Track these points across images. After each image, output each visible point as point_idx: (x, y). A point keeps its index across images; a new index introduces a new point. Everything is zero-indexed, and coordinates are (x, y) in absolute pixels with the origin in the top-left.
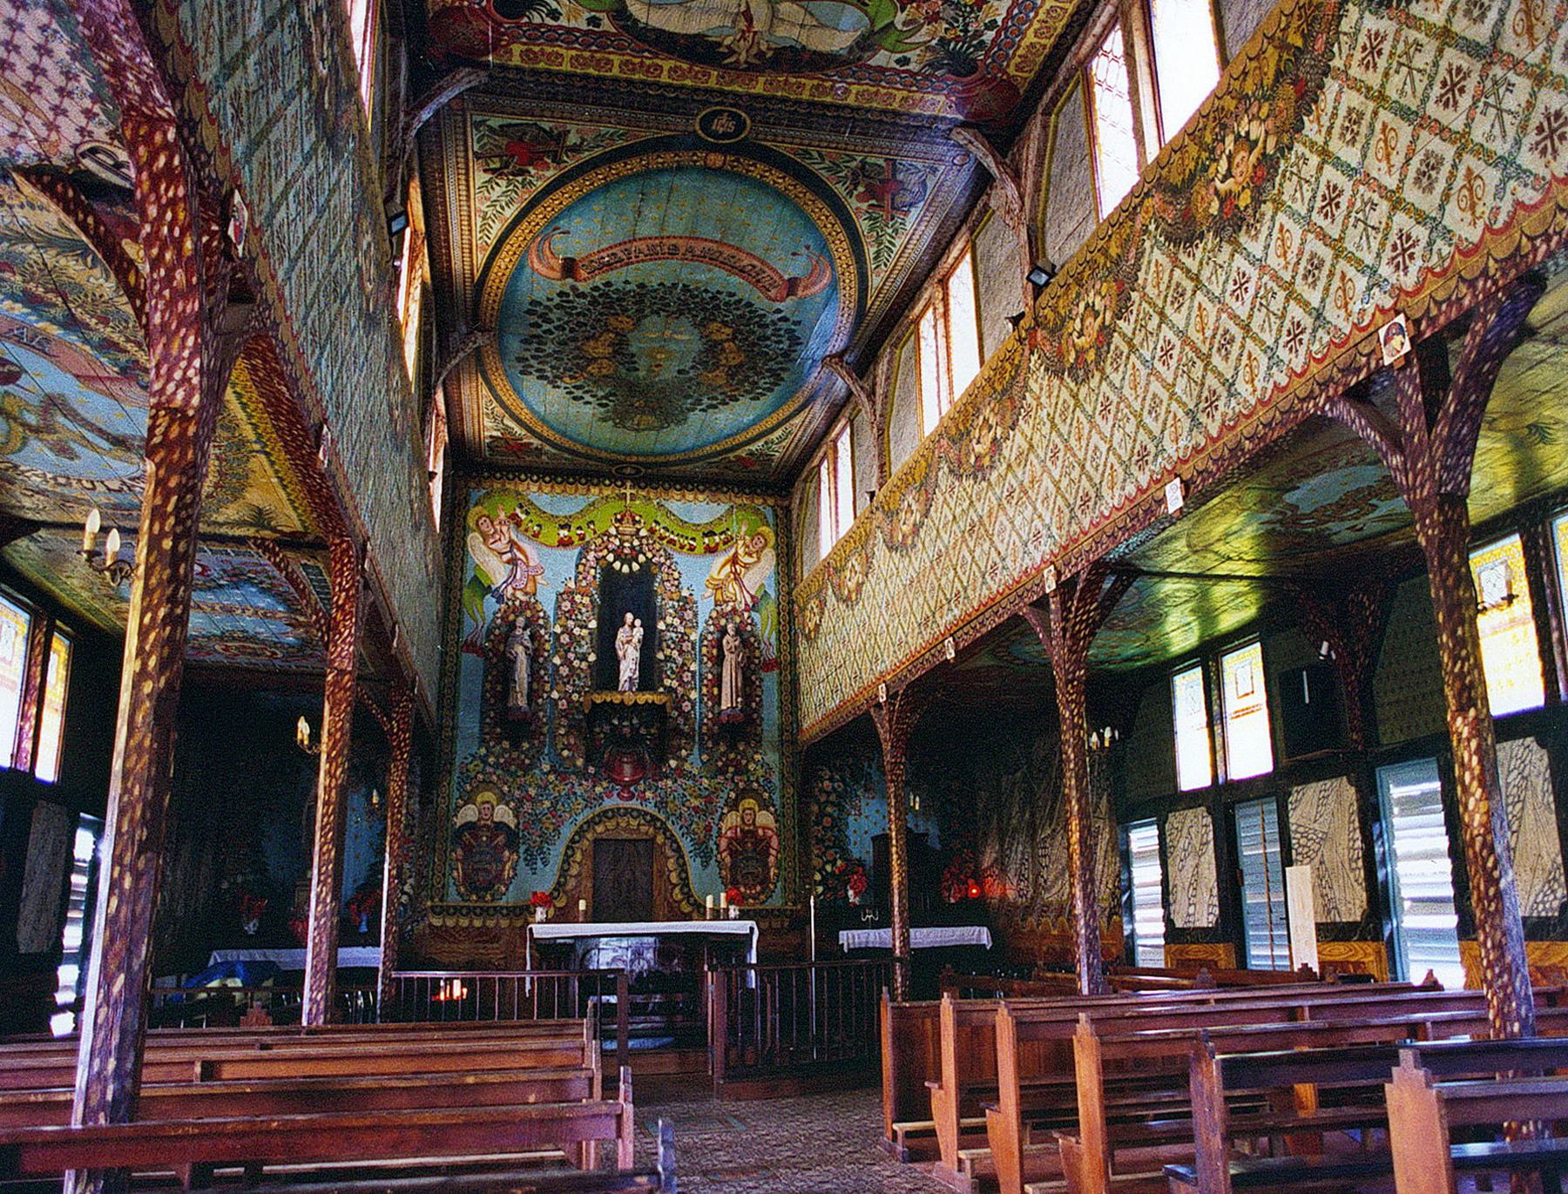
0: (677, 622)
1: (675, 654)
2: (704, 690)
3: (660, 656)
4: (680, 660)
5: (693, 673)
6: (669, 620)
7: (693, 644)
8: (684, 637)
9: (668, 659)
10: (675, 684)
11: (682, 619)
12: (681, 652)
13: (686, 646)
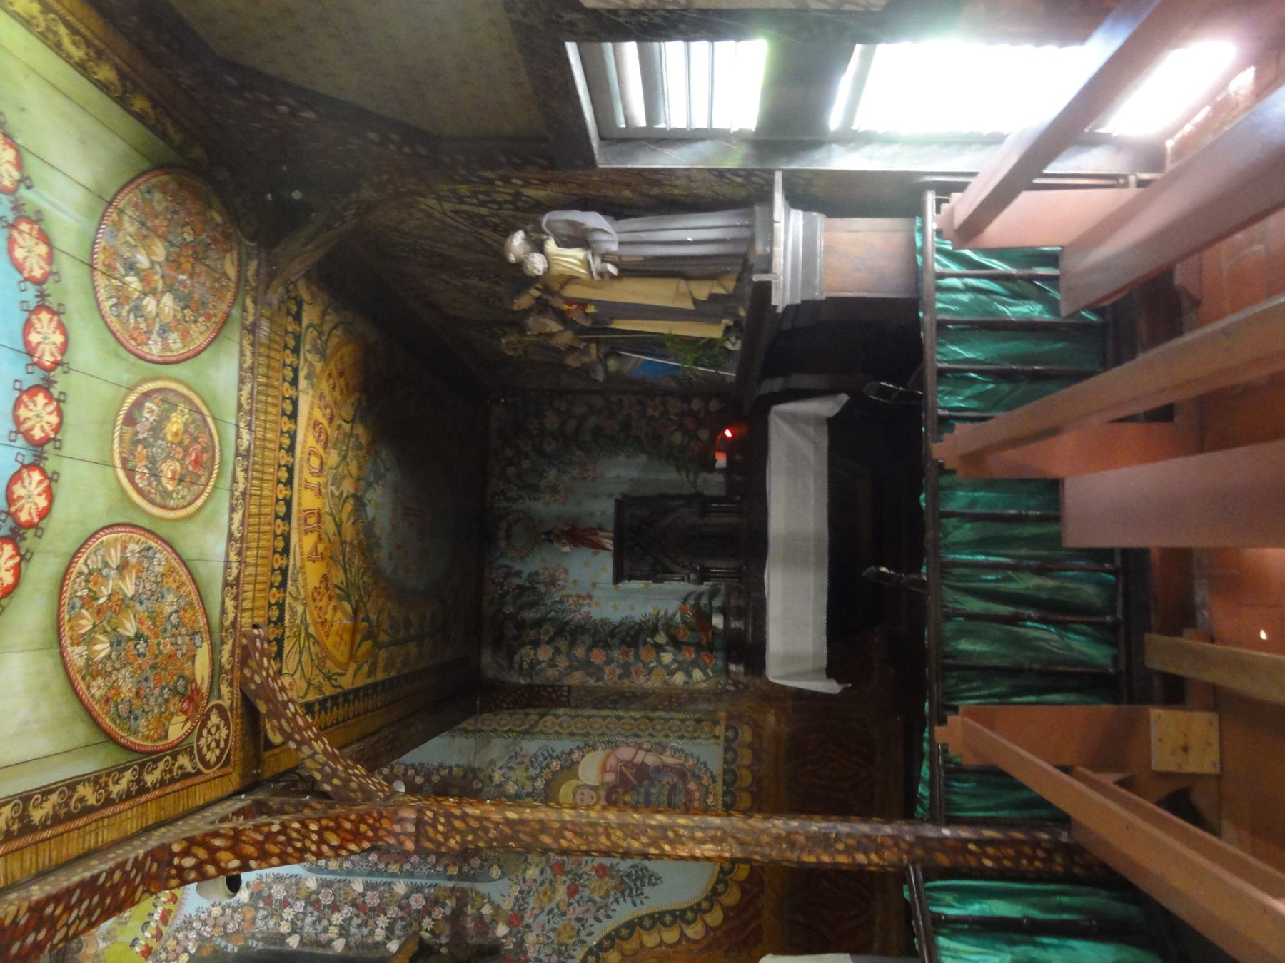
0: (288, 914)
1: (337, 918)
2: (394, 868)
3: (339, 945)
4: (347, 910)
5: (368, 887)
6: (285, 928)
7: (326, 884)
8: (312, 902)
9: (344, 931)
10: (382, 921)
11: (285, 903)
12: (335, 907)
13: (326, 898)
